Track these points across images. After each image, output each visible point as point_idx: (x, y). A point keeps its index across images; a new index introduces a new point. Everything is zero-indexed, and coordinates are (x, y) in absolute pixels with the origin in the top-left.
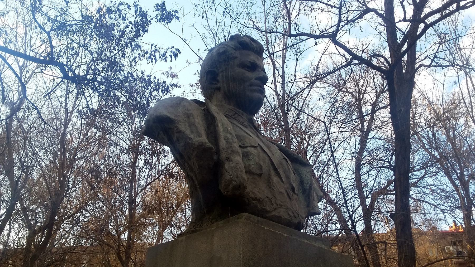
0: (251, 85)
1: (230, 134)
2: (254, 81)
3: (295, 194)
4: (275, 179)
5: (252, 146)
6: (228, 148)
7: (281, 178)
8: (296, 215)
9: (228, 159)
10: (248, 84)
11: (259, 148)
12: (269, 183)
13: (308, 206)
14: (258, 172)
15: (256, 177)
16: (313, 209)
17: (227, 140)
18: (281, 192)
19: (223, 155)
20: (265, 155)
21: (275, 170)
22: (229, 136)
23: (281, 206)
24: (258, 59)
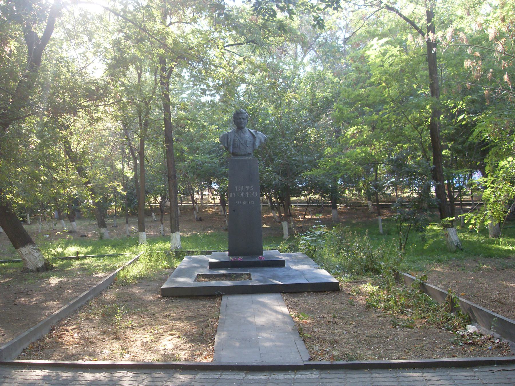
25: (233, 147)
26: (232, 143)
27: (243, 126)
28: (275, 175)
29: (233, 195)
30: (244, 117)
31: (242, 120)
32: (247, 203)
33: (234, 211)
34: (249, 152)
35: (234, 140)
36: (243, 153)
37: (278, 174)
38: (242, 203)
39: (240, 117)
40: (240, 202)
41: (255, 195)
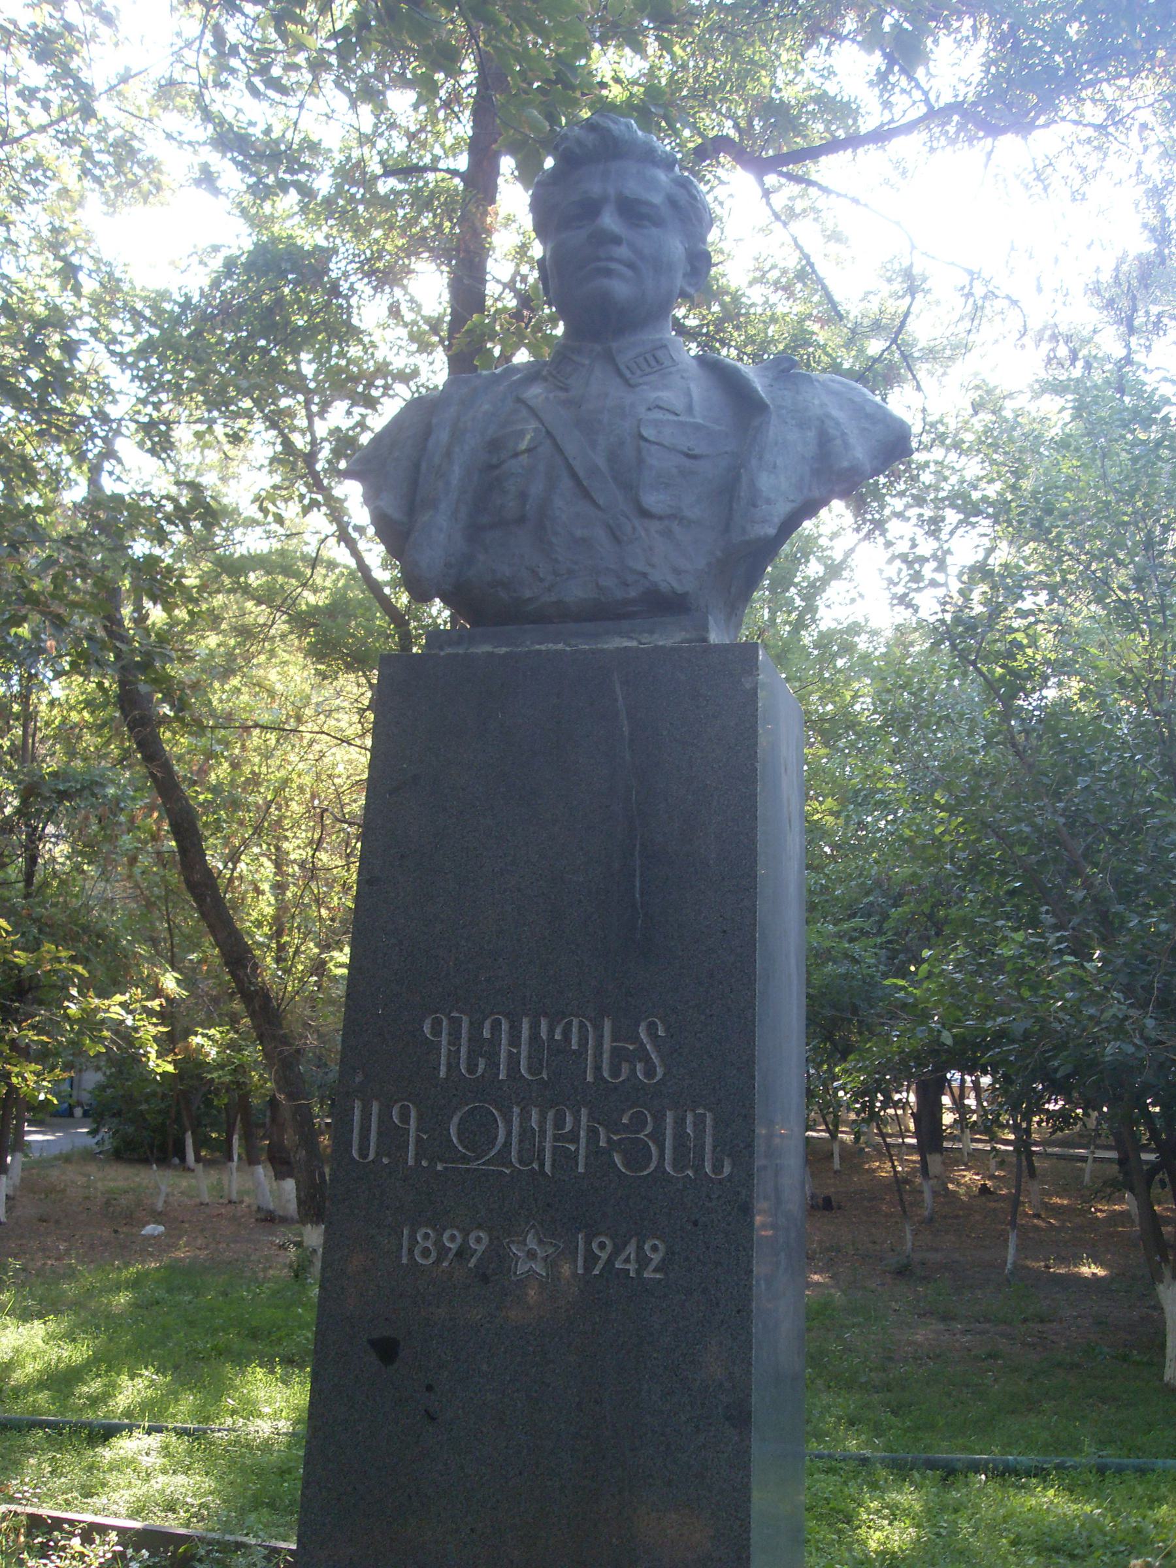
3: (660, 518)
7: (594, 502)
25: (474, 532)
26: (456, 473)
27: (621, 289)
28: (1117, 1005)
29: (392, 1137)
30: (633, 188)
31: (609, 220)
33: (387, 1350)
34: (664, 579)
35: (494, 445)
36: (577, 592)
37: (1143, 1006)
39: (595, 188)
40: (480, 1242)
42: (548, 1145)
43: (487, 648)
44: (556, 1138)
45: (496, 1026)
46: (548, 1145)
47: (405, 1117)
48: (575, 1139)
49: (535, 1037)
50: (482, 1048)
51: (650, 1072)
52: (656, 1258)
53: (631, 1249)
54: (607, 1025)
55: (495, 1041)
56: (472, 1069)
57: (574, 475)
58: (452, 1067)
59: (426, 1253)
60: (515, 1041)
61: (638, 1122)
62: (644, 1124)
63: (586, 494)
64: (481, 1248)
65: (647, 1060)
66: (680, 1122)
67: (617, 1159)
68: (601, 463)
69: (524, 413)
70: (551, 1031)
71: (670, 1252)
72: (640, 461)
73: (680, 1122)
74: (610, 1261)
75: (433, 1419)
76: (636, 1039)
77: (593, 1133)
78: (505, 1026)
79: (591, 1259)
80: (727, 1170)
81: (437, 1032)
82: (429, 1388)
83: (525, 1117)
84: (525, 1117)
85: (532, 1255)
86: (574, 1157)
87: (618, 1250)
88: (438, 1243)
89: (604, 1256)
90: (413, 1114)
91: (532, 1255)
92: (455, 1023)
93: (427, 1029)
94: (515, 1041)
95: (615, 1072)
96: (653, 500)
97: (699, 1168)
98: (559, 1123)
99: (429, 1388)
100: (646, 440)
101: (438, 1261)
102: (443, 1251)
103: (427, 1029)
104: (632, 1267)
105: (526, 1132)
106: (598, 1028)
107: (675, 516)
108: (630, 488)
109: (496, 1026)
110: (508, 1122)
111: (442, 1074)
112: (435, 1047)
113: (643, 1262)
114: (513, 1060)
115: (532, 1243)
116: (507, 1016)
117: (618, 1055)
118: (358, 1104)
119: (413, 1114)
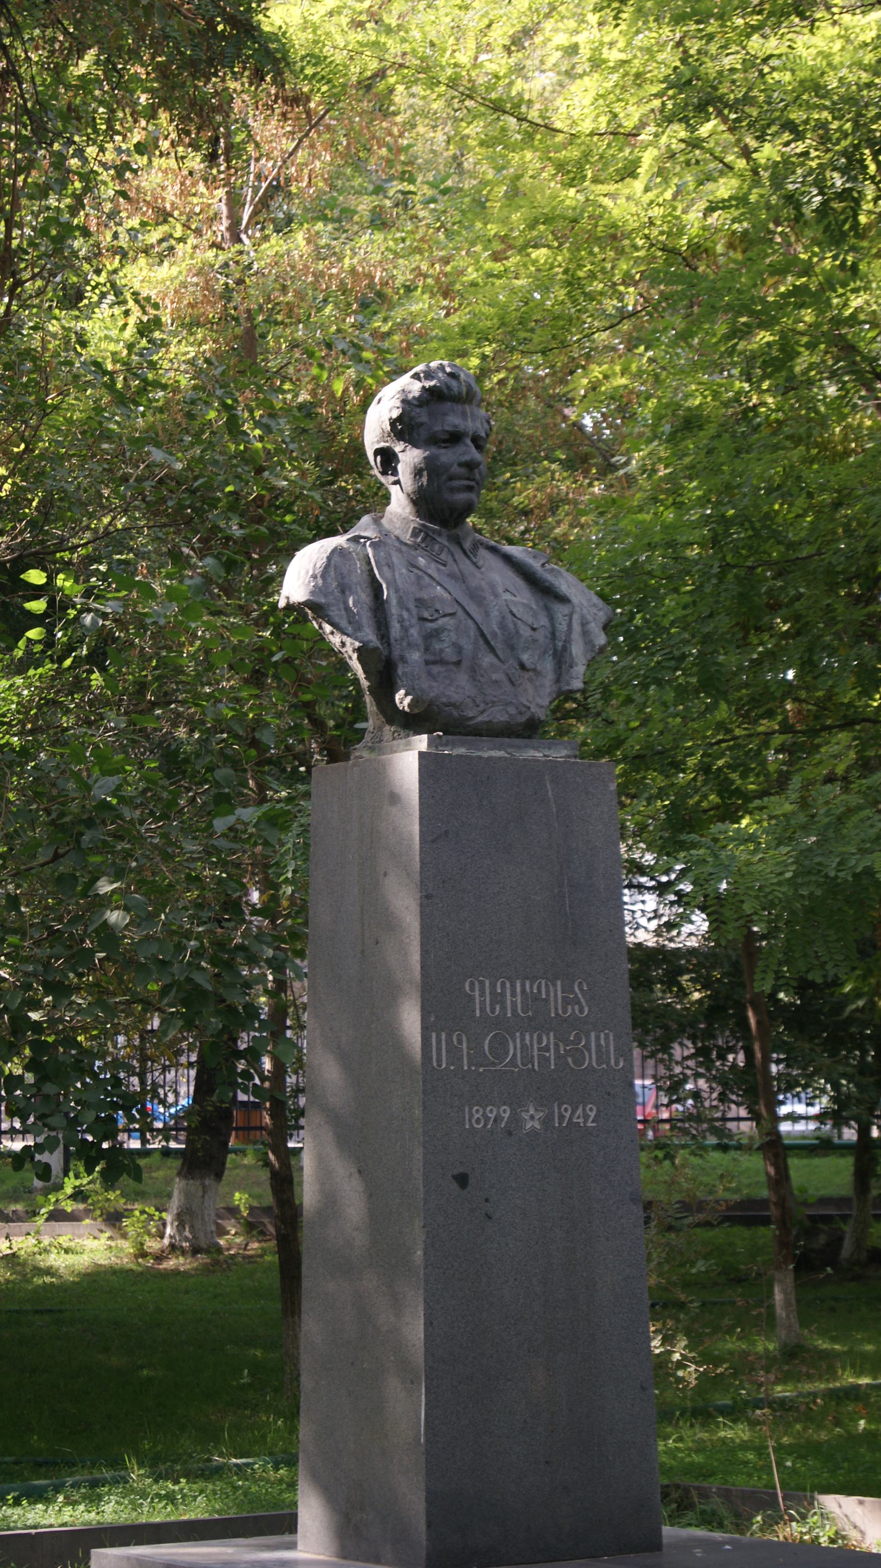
0: (451, 478)
1: (408, 610)
2: (456, 470)
4: (487, 659)
5: (445, 616)
6: (402, 639)
8: (523, 709)
9: (403, 659)
10: (444, 478)
11: (460, 613)
12: (474, 671)
13: (558, 680)
14: (455, 659)
15: (452, 667)
16: (568, 684)
17: (401, 621)
18: (496, 682)
19: (396, 653)
20: (470, 622)
21: (487, 642)
22: (405, 615)
23: (493, 702)
24: (464, 415)
32: (547, 1122)
33: (462, 1180)
36: (499, 715)
38: (515, 1119)
41: (602, 1055)
42: (536, 1053)
43: (462, 751)
44: (539, 1049)
45: (503, 985)
46: (536, 1053)
47: (460, 1042)
48: (548, 1050)
49: (523, 991)
50: (498, 999)
51: (581, 1011)
52: (592, 1115)
53: (580, 1111)
54: (559, 983)
55: (503, 994)
56: (493, 1011)
57: (483, 635)
58: (482, 1010)
59: (478, 1121)
60: (513, 994)
61: (578, 1039)
62: (580, 1040)
63: (492, 650)
64: (507, 1115)
65: (579, 1003)
66: (598, 1038)
67: (570, 1060)
68: (495, 628)
69: (427, 579)
70: (531, 987)
71: (598, 1111)
72: (517, 632)
73: (598, 1038)
74: (570, 1119)
75: (489, 1217)
76: (573, 992)
77: (557, 1045)
78: (508, 985)
79: (561, 1117)
80: (621, 1064)
81: (472, 989)
82: (487, 1200)
83: (523, 1040)
84: (523, 1040)
85: (532, 1117)
86: (548, 1060)
87: (573, 1113)
88: (484, 1115)
89: (568, 1115)
90: (464, 1038)
91: (532, 1117)
92: (482, 983)
93: (467, 988)
94: (513, 994)
95: (565, 1011)
96: (525, 657)
97: (608, 1063)
98: (540, 1042)
99: (487, 1200)
100: (514, 615)
101: (485, 1125)
102: (487, 1119)
103: (467, 988)
104: (581, 1120)
105: (524, 1047)
106: (555, 985)
107: (534, 670)
108: (512, 648)
109: (503, 985)
110: (514, 1041)
111: (478, 1013)
112: (471, 999)
113: (586, 1117)
114: (514, 1004)
115: (532, 1112)
116: (508, 978)
117: (566, 1001)
118: (434, 1035)
119: (464, 1038)
